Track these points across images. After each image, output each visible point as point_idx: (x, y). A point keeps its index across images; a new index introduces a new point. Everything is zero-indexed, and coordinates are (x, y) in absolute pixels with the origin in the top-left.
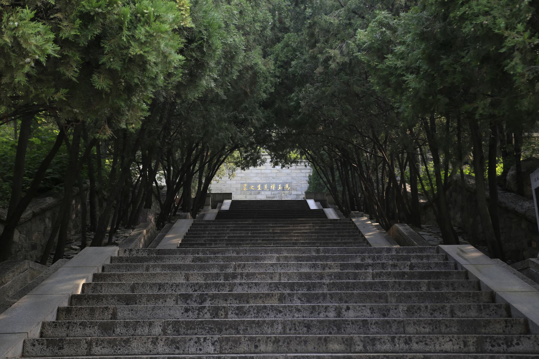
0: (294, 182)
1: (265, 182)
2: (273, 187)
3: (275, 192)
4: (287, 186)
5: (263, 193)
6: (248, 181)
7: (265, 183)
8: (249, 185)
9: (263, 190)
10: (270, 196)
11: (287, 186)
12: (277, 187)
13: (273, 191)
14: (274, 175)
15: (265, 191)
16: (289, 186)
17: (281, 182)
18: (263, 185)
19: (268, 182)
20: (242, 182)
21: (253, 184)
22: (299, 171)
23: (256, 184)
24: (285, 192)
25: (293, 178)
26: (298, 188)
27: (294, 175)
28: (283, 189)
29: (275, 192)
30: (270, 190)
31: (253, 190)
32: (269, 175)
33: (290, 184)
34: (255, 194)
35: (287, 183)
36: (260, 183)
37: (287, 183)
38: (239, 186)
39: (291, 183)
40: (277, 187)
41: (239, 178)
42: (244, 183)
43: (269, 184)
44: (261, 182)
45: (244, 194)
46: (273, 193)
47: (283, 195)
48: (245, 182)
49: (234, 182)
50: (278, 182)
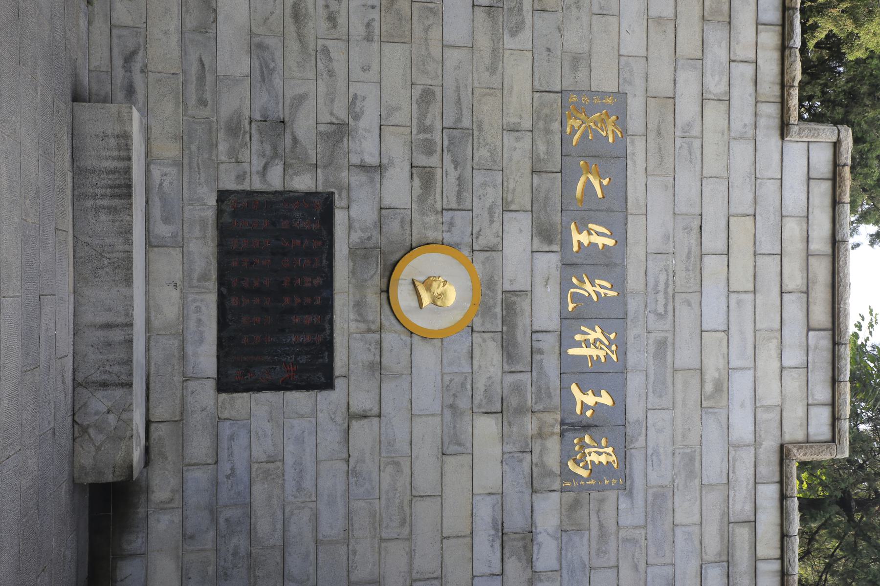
0: (630, 513)
1: (634, 280)
2: (592, 345)
3: (551, 365)
4: (601, 455)
5: (548, 263)
6: (637, 149)
7: (619, 284)
8: (611, 159)
9: (575, 264)
10: (523, 323)
11: (601, 455)
12: (590, 375)
13: (564, 340)
14: (685, 356)
15: (565, 285)
16: (596, 470)
17: (635, 411)
18: (606, 263)
19: (633, 305)
20: (635, 105)
21: (618, 189)
22: (713, 546)
23: (613, 211)
24: (553, 444)
25: (660, 501)
26: (581, 548)
27: (685, 510)
28: (575, 426)
29: (551, 365)
30: (572, 320)
31: (568, 185)
32: (686, 317)
33: (616, 478)
34: (537, 204)
35: (623, 454)
36: (622, 241)
37: (623, 454)
38: (604, 79)
39: (626, 488)
40: (590, 375)
41: (661, 84)
42: (622, 121)
43: (612, 316)
44: (635, 252)
45: (536, 114)
46: (549, 343)
47: (530, 425)
48: (635, 124)
49: (633, 44)
50: (635, 382)
